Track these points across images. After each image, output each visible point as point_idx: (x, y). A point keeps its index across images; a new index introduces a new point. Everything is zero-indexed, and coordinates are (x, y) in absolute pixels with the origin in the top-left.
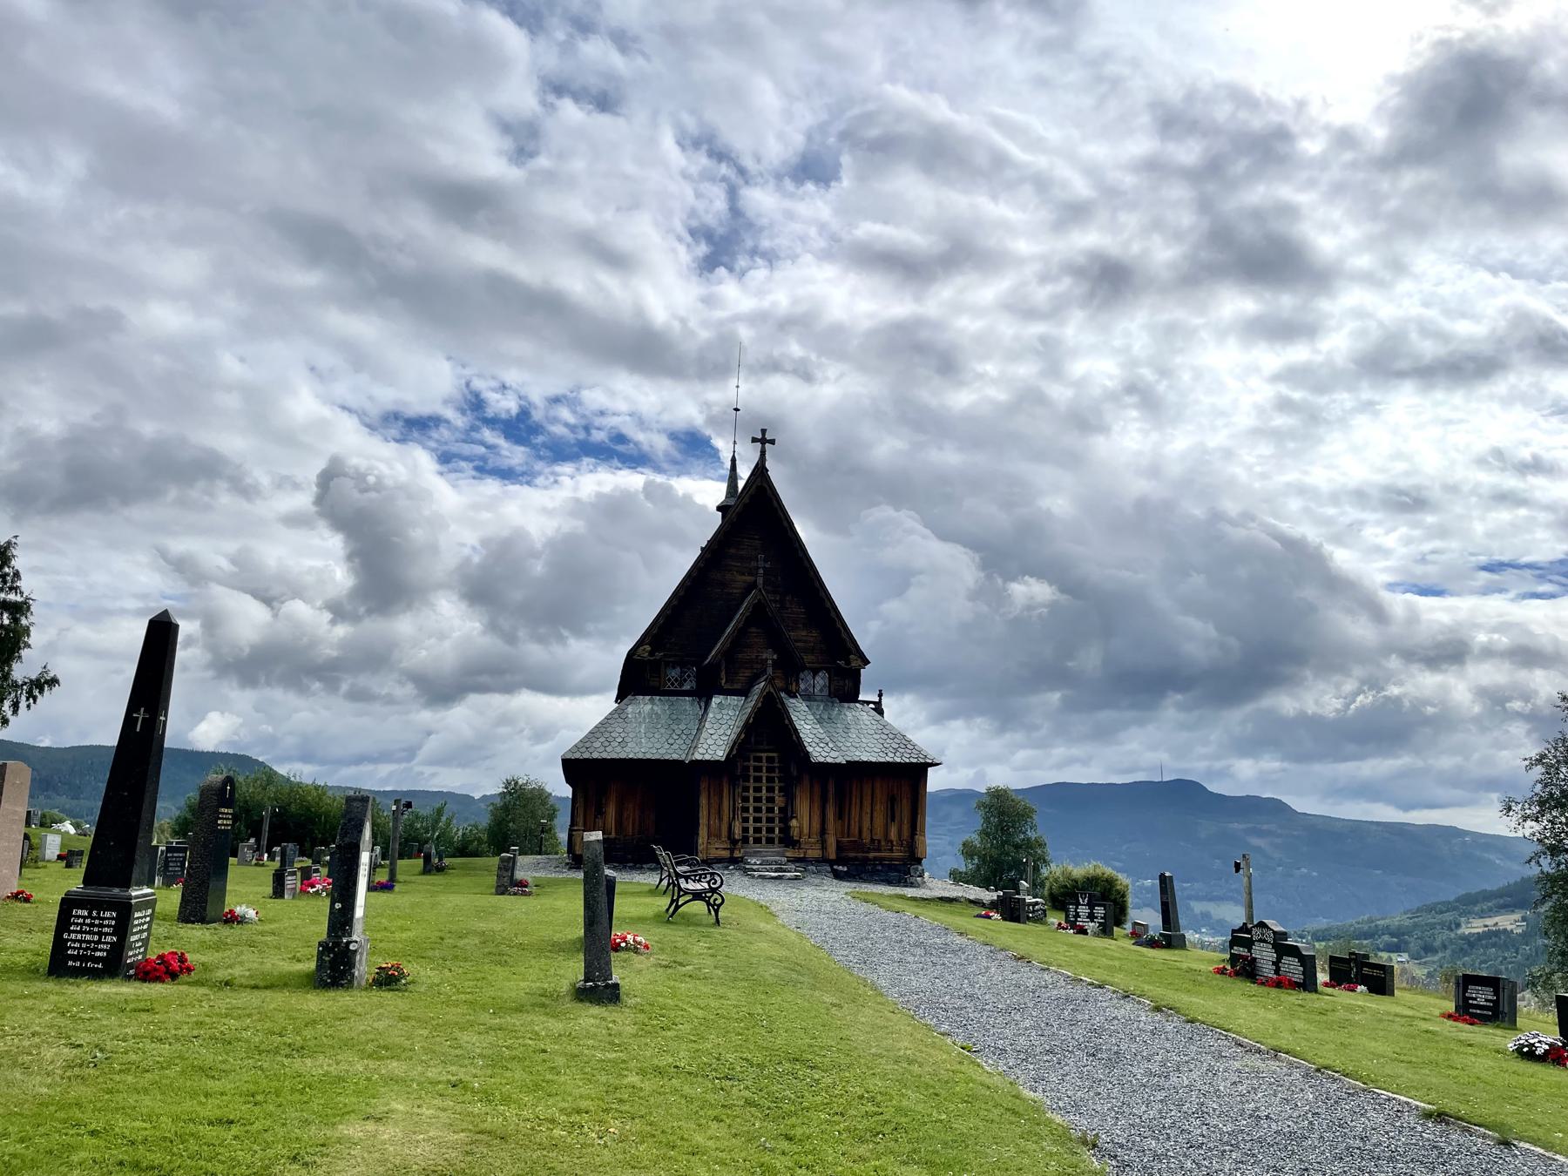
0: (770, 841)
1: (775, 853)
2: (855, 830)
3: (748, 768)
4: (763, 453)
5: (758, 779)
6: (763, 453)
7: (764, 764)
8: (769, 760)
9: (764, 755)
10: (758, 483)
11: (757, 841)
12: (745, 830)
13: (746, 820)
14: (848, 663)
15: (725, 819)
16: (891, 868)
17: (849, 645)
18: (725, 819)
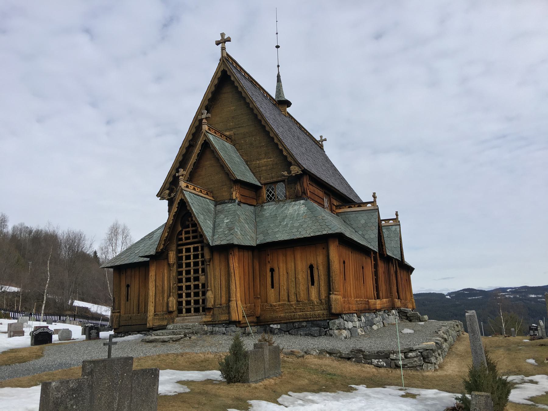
0: (197, 310)
1: (193, 321)
2: (284, 293)
3: (180, 258)
4: (223, 49)
5: (188, 265)
6: (223, 49)
7: (192, 253)
8: (196, 249)
9: (191, 246)
10: (222, 69)
11: (188, 311)
12: (180, 303)
13: (180, 296)
14: (290, 172)
15: (166, 295)
16: (313, 322)
17: (289, 159)
18: (166, 295)
